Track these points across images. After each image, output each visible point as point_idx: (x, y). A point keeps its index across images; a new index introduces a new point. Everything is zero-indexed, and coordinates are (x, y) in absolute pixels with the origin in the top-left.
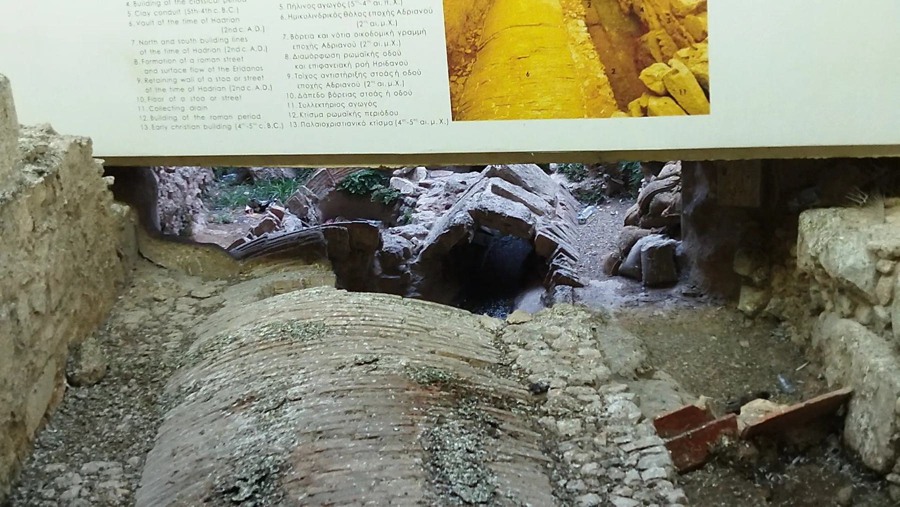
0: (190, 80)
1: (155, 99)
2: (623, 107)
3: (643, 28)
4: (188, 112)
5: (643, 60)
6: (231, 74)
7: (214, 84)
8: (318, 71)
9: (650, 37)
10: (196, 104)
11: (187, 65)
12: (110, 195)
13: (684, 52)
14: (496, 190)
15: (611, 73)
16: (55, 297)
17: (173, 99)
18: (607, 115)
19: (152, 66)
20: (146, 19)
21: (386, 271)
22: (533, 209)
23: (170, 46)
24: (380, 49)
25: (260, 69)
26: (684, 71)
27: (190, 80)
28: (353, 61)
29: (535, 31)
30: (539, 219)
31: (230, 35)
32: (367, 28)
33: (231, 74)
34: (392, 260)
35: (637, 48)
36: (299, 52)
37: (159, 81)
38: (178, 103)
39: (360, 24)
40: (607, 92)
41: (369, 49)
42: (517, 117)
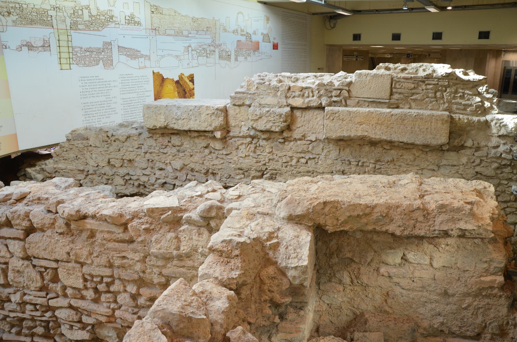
0: (97, 113)
1: (88, 120)
4: (96, 123)
6: (108, 110)
7: (104, 114)
8: (128, 107)
10: (99, 120)
11: (97, 109)
17: (92, 120)
19: (87, 110)
20: (85, 96)
23: (92, 104)
24: (142, 101)
25: (115, 108)
27: (97, 113)
28: (136, 104)
31: (108, 100)
32: (139, 96)
33: (108, 110)
36: (124, 103)
37: (88, 115)
38: (94, 121)
39: (138, 95)
41: (140, 100)
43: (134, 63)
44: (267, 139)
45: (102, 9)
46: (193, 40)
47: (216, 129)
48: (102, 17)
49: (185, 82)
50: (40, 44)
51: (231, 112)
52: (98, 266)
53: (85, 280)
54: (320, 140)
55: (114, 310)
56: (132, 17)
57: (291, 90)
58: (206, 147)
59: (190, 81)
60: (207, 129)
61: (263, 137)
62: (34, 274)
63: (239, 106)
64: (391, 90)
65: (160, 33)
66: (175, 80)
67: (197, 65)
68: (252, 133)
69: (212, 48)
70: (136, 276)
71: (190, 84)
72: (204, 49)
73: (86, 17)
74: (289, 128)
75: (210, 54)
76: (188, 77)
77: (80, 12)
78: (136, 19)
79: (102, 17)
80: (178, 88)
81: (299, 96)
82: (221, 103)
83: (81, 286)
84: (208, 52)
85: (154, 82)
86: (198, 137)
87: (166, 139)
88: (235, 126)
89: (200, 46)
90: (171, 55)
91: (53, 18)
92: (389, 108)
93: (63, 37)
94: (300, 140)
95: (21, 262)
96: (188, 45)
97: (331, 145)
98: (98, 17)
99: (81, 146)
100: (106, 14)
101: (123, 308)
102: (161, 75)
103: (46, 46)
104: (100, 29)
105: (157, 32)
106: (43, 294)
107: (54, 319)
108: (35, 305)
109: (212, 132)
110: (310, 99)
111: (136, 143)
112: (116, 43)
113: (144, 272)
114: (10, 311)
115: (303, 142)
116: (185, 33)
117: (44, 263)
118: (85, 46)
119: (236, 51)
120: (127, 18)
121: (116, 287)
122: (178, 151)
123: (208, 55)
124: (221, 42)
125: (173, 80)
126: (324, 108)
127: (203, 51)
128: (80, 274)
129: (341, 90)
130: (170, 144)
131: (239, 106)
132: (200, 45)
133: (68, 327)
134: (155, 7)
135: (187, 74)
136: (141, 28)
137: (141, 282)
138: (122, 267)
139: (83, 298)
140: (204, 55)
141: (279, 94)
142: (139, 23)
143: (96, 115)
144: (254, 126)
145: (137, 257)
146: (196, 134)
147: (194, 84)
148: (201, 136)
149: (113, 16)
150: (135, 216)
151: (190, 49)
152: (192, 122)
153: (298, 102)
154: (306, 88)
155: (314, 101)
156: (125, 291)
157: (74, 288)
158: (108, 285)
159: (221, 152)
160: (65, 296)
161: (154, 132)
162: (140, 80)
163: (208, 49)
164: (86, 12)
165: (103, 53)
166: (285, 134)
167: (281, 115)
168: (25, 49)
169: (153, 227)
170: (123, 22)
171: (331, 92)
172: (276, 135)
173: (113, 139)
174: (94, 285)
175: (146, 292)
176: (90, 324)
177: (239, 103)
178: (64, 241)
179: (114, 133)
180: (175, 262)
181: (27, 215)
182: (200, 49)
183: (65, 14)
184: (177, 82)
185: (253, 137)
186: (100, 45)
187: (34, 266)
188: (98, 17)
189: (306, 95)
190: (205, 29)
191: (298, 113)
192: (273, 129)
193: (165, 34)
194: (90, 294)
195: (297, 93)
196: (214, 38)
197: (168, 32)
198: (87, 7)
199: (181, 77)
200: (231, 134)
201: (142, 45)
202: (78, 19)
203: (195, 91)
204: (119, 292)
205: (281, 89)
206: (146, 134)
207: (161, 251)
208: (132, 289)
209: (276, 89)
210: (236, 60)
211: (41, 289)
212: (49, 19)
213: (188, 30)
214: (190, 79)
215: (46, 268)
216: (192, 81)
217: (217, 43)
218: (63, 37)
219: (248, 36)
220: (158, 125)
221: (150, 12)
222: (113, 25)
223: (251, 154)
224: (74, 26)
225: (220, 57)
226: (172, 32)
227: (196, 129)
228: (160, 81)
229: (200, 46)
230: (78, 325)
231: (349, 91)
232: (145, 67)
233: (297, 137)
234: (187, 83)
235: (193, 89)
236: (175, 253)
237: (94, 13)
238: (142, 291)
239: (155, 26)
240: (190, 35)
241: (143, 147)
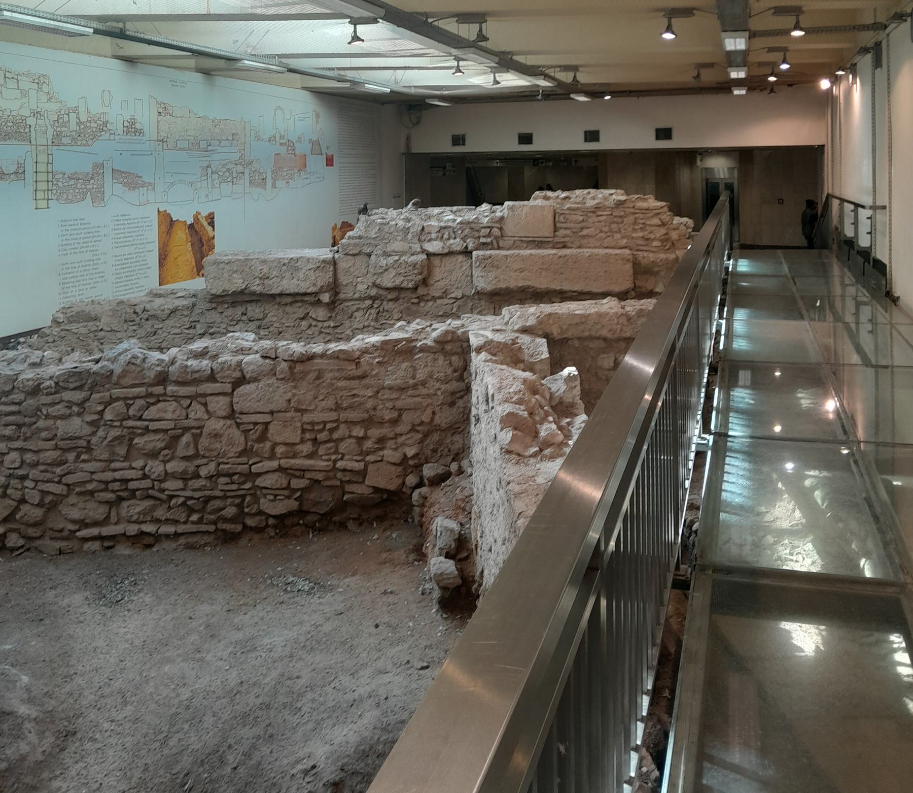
44: (396, 300)
45: (93, 112)
47: (321, 291)
48: (93, 125)
49: (202, 226)
50: (13, 169)
51: (342, 265)
52: (323, 410)
53: (304, 431)
54: (468, 297)
55: (335, 461)
56: (133, 122)
57: (426, 230)
58: (303, 319)
60: (309, 291)
61: (390, 297)
62: (236, 433)
63: (354, 255)
64: (555, 225)
66: (188, 223)
68: (373, 292)
69: (240, 168)
70: (366, 416)
72: (229, 170)
73: (73, 126)
74: (425, 282)
77: (66, 118)
78: (138, 126)
79: (93, 125)
80: (191, 236)
81: (436, 239)
82: (325, 253)
83: (298, 440)
84: (235, 175)
86: (291, 303)
87: (239, 310)
88: (347, 285)
89: (223, 166)
91: (32, 128)
92: (554, 248)
93: (43, 158)
94: (440, 298)
95: (222, 422)
96: (206, 164)
97: (483, 303)
98: (88, 124)
99: (83, 331)
101: (346, 457)
104: (90, 142)
106: (244, 459)
107: (252, 491)
108: (230, 475)
109: (316, 294)
110: (452, 241)
111: (187, 319)
113: (375, 409)
114: (194, 490)
115: (445, 301)
117: (253, 418)
119: (273, 172)
120: (126, 124)
121: (342, 431)
122: (259, 327)
126: (471, 252)
127: (227, 174)
128: (299, 425)
129: (491, 228)
130: (244, 318)
131: (354, 255)
133: (272, 497)
134: (163, 106)
137: (368, 422)
138: (351, 407)
139: (295, 456)
141: (410, 236)
142: (141, 132)
143: (77, 284)
144: (378, 282)
145: (369, 393)
146: (290, 299)
148: (296, 302)
149: (107, 122)
150: (365, 351)
151: (209, 170)
152: (285, 282)
153: (434, 247)
154: (445, 228)
155: (456, 244)
156: (350, 436)
157: (286, 444)
158: (332, 431)
159: (326, 324)
160: (272, 456)
161: (221, 300)
163: (234, 170)
164: (73, 116)
165: (92, 181)
166: (421, 291)
167: (414, 265)
169: (386, 359)
170: (120, 131)
171: (478, 231)
172: (409, 294)
173: (145, 315)
174: (313, 437)
175: (375, 433)
176: (298, 490)
177: (354, 252)
178: (283, 387)
179: (148, 306)
180: (410, 392)
181: (239, 363)
182: (224, 170)
183: (47, 122)
185: (374, 299)
187: (238, 425)
188: (88, 124)
189: (446, 236)
190: (230, 138)
191: (436, 261)
192: (405, 285)
193: (176, 148)
194: (306, 448)
195: (434, 236)
198: (76, 110)
200: (342, 296)
202: (63, 129)
204: (342, 439)
205: (412, 231)
206: (203, 306)
207: (399, 381)
208: (358, 432)
209: (406, 231)
210: (274, 186)
211: (241, 454)
212: (27, 130)
213: (207, 141)
215: (256, 424)
216: (212, 224)
218: (43, 158)
219: (290, 145)
220: (232, 289)
222: (105, 136)
223: (372, 324)
225: (250, 183)
226: (185, 145)
227: (292, 291)
229: (223, 166)
230: (286, 492)
231: (501, 229)
233: (437, 295)
236: (411, 382)
237: (83, 118)
238: (369, 433)
239: (163, 134)
240: (209, 148)
241: (198, 326)
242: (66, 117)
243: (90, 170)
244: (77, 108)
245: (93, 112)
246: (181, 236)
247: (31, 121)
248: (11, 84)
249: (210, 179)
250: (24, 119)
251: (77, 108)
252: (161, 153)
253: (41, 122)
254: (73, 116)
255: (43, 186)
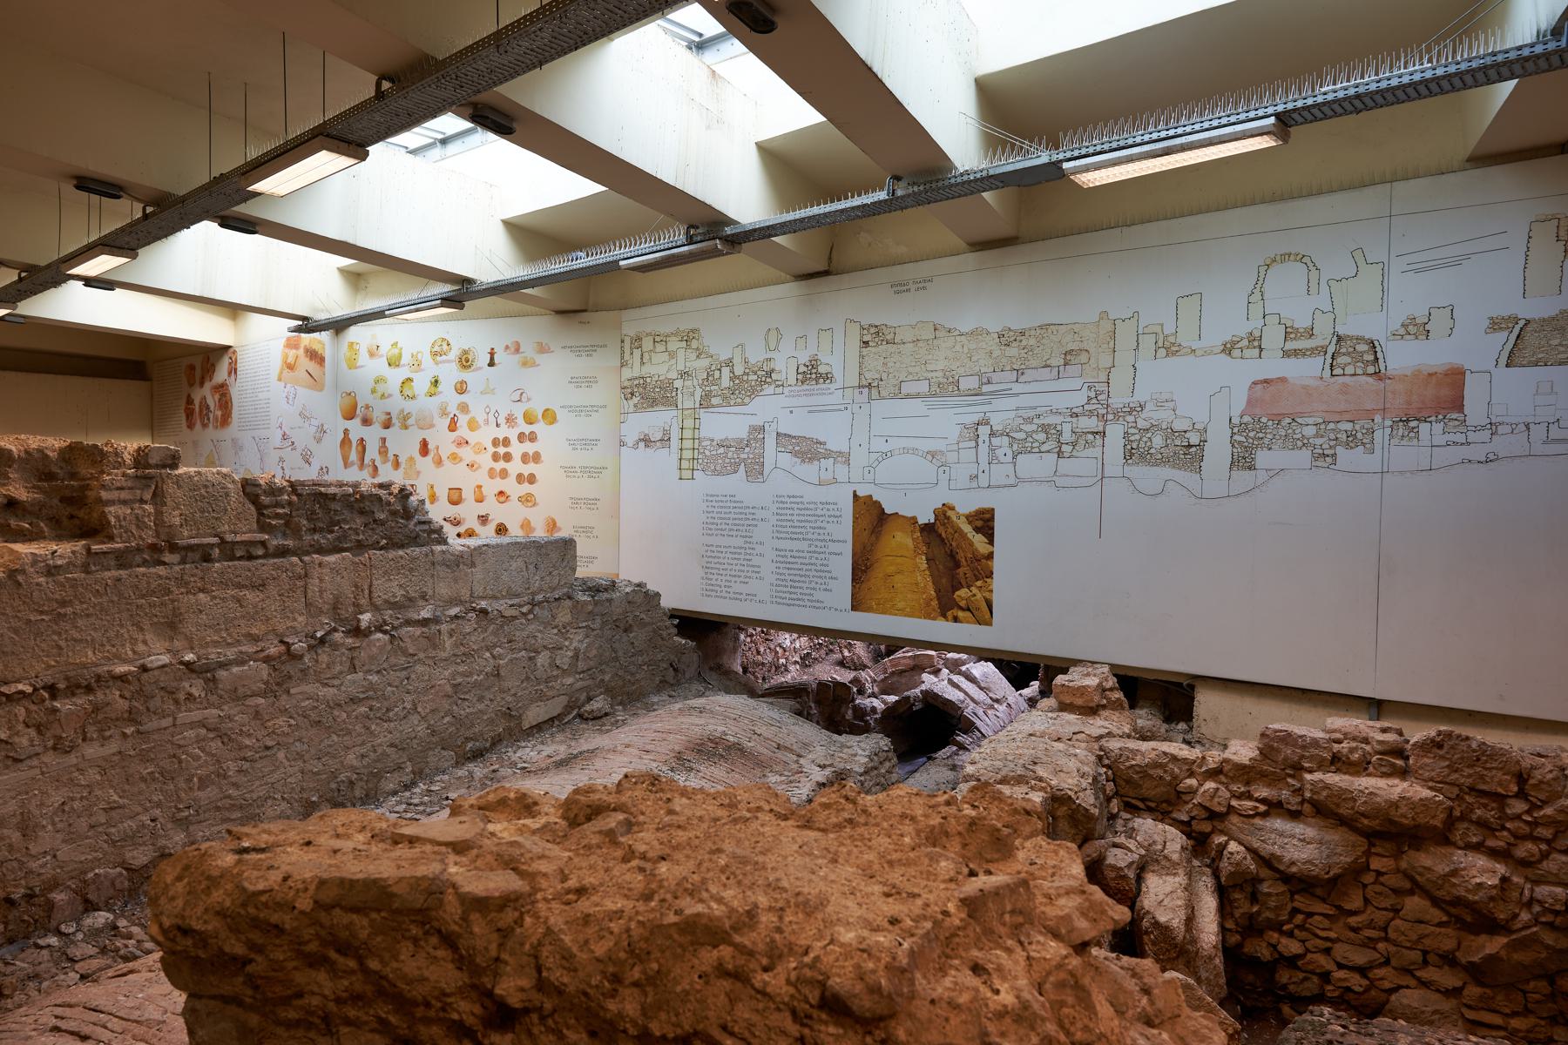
2: (945, 616)
3: (957, 565)
5: (956, 587)
9: (961, 571)
12: (675, 631)
13: (979, 583)
14: (951, 682)
15: (938, 591)
16: (581, 665)
18: (934, 619)
21: (855, 717)
22: (973, 700)
26: (979, 596)
29: (899, 560)
30: (972, 705)
34: (860, 713)
35: (953, 577)
40: (935, 603)
42: (884, 613)
43: (809, 471)
46: (1000, 403)
49: (958, 531)
56: (813, 364)
59: (977, 530)
65: (883, 393)
66: (922, 520)
67: (1012, 481)
69: (1091, 423)
71: (979, 541)
72: (1045, 428)
73: (726, 382)
75: (1074, 445)
76: (970, 518)
78: (822, 369)
80: (928, 544)
84: (1067, 436)
85: (856, 519)
89: (1029, 420)
90: (915, 451)
93: (689, 423)
100: (761, 369)
102: (878, 505)
103: (665, 440)
104: (747, 400)
105: (874, 391)
112: (774, 426)
116: (968, 383)
118: (718, 437)
119: (1237, 428)
120: (802, 369)
123: (1065, 448)
124: (1141, 396)
125: (914, 520)
127: (1041, 436)
132: (1032, 413)
134: (873, 330)
135: (966, 504)
136: (833, 387)
140: (1044, 448)
142: (827, 377)
147: (991, 542)
149: (773, 371)
162: (819, 512)
163: (1067, 429)
164: (726, 371)
168: (642, 444)
170: (792, 381)
182: (1029, 428)
184: (928, 529)
186: (744, 435)
193: (898, 395)
196: (1103, 387)
197: (906, 389)
198: (729, 363)
199: (943, 514)
201: (832, 431)
203: (997, 565)
210: (1243, 460)
213: (979, 375)
214: (979, 523)
217: (1117, 401)
221: (857, 343)
222: (769, 389)
224: (705, 402)
225: (1129, 455)
226: (923, 387)
228: (872, 519)
229: (1029, 420)
232: (835, 481)
234: (963, 535)
235: (990, 556)
240: (985, 389)
242: (717, 374)
243: (744, 435)
244: (731, 360)
245: (752, 361)
246: (900, 541)
247: (678, 384)
248: (660, 347)
249: (983, 449)
250: (671, 382)
251: (731, 360)
252: (866, 407)
253: (688, 383)
254: (726, 371)
255: (688, 454)
